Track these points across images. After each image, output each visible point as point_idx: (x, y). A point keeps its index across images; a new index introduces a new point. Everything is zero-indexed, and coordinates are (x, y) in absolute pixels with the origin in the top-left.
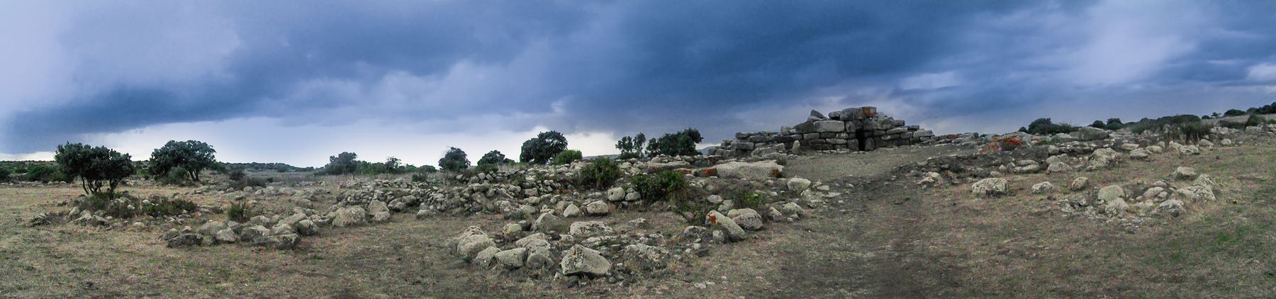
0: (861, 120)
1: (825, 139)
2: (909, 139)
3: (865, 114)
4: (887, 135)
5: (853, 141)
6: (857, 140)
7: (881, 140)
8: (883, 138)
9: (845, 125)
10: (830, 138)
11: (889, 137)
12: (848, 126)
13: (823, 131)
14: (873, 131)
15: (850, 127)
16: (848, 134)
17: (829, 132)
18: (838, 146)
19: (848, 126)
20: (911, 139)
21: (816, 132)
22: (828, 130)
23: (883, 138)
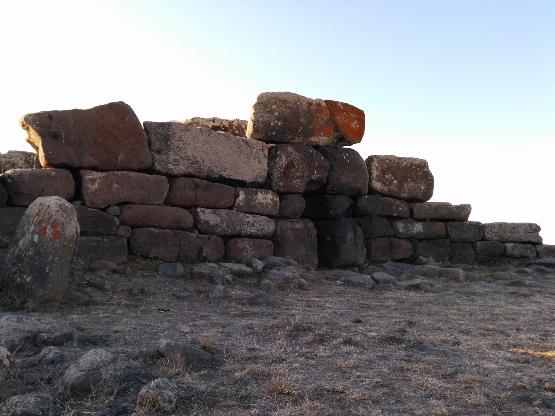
0: (317, 147)
1: (190, 207)
2: (473, 244)
3: (337, 128)
4: (412, 217)
5: (299, 225)
6: (311, 224)
7: (395, 236)
8: (401, 227)
9: (272, 156)
10: (214, 208)
11: (418, 228)
12: (283, 161)
13: (181, 169)
14: (355, 196)
15: (290, 165)
16: (280, 194)
17: (209, 178)
18: (244, 244)
19: (283, 161)
20: (479, 244)
21: (150, 170)
22: (217, 171)
23: (401, 227)
